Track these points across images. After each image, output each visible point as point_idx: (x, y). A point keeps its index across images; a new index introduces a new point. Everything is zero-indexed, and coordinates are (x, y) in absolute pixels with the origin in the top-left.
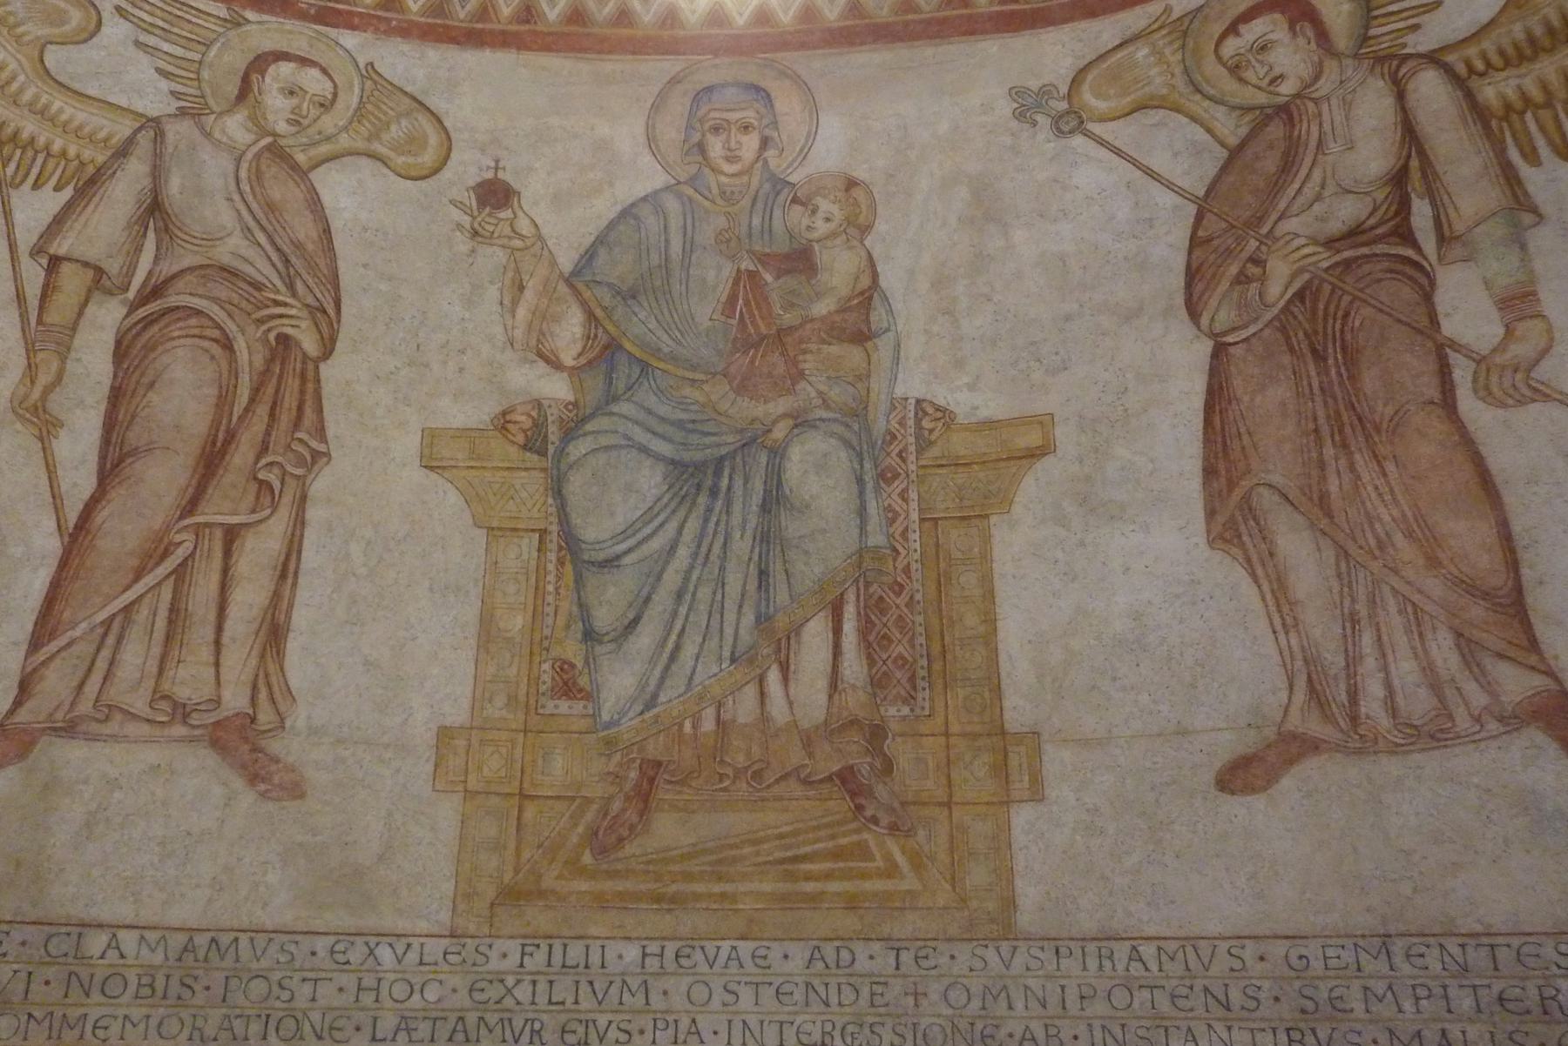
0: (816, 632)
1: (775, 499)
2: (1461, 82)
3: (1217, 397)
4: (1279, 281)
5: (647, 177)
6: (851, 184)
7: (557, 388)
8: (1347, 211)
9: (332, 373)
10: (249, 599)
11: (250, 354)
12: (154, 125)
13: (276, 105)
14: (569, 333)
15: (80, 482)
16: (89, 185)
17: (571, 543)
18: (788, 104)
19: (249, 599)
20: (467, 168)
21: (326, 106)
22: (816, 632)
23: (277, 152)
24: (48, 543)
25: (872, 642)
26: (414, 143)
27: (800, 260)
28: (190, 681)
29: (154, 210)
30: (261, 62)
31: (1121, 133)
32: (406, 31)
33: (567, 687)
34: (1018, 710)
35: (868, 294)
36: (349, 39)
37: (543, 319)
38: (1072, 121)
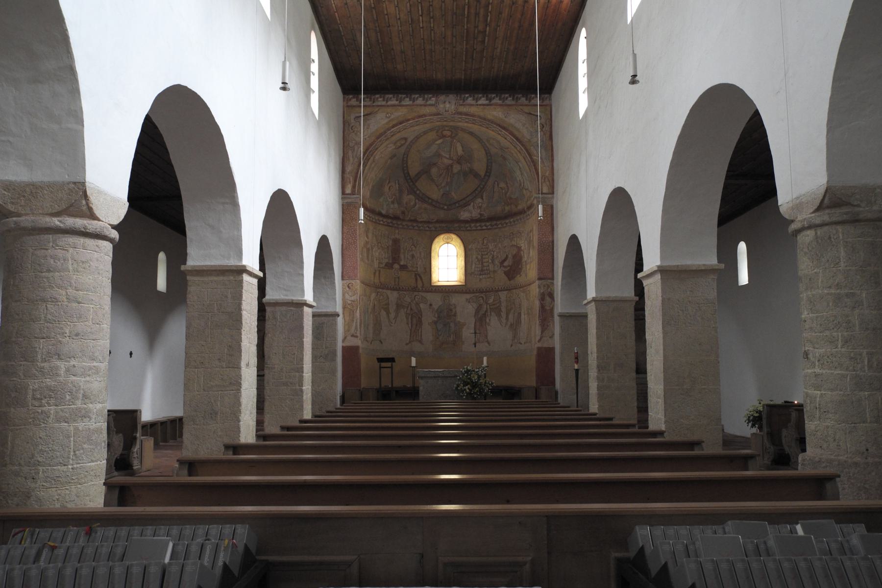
0: (452, 335)
1: (450, 327)
2: (490, 305)
3: (475, 323)
4: (479, 316)
5: (441, 303)
6: (454, 305)
7: (436, 319)
8: (483, 312)
9: (422, 319)
10: (420, 334)
11: (418, 318)
12: (410, 303)
13: (416, 299)
14: (436, 316)
15: (410, 328)
16: (408, 307)
17: (437, 329)
18: (450, 298)
19: (420, 334)
20: (429, 303)
21: (419, 299)
22: (452, 335)
23: (417, 303)
24: (409, 331)
25: (455, 336)
26: (425, 301)
27: (451, 310)
28: (417, 338)
29: (411, 309)
30: (415, 296)
31: (472, 303)
32: (424, 292)
33: (438, 338)
34: (463, 340)
35: (456, 313)
36: (420, 293)
37: (435, 315)
38: (469, 302)
